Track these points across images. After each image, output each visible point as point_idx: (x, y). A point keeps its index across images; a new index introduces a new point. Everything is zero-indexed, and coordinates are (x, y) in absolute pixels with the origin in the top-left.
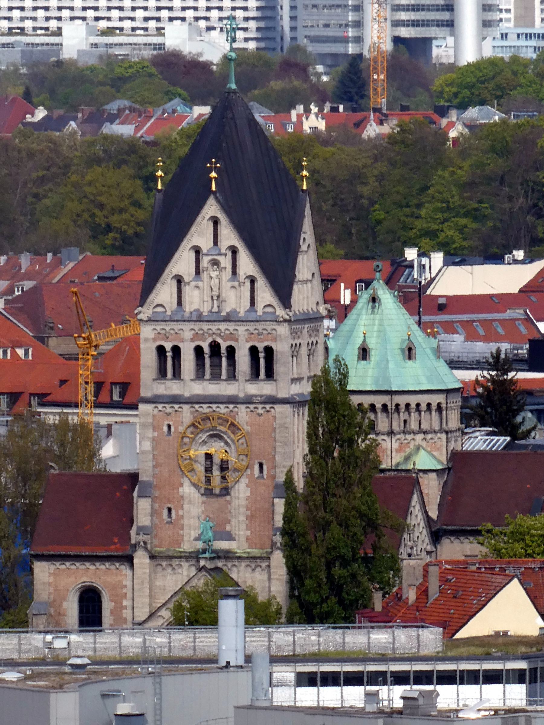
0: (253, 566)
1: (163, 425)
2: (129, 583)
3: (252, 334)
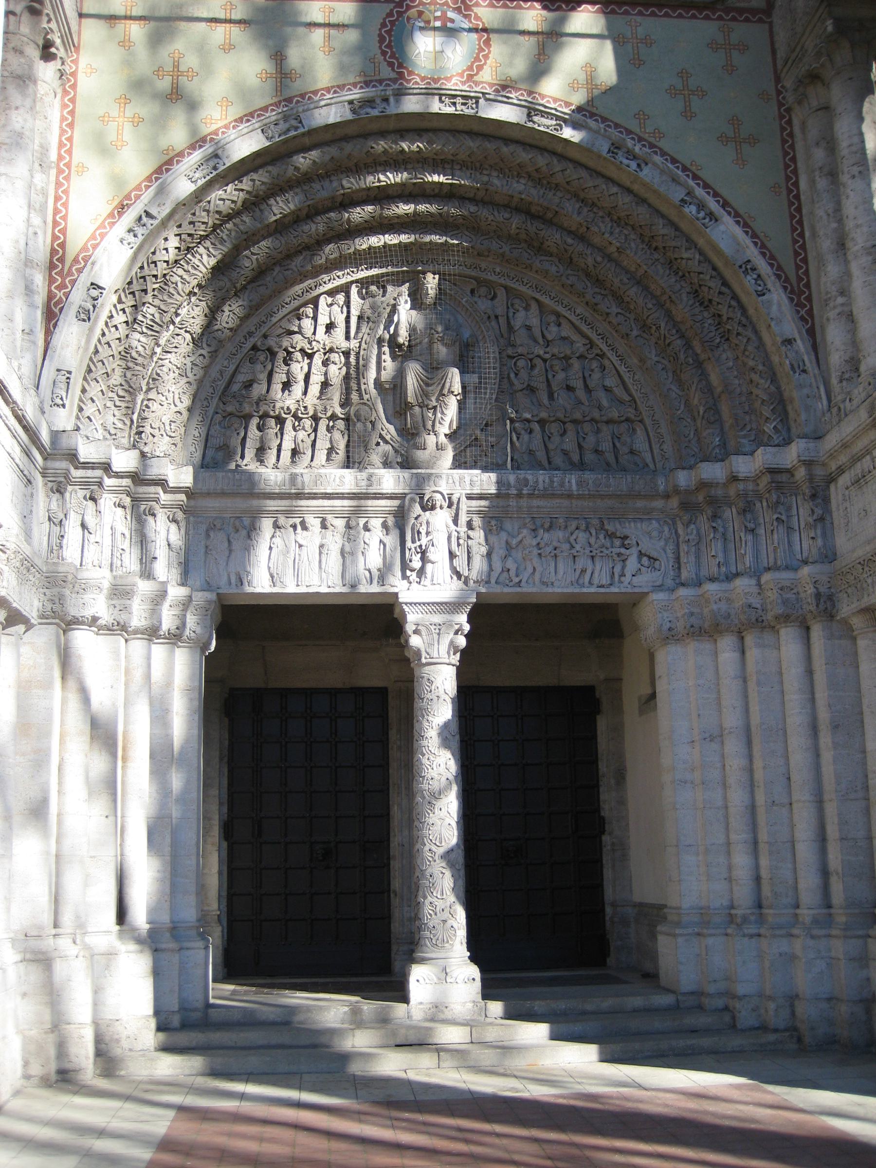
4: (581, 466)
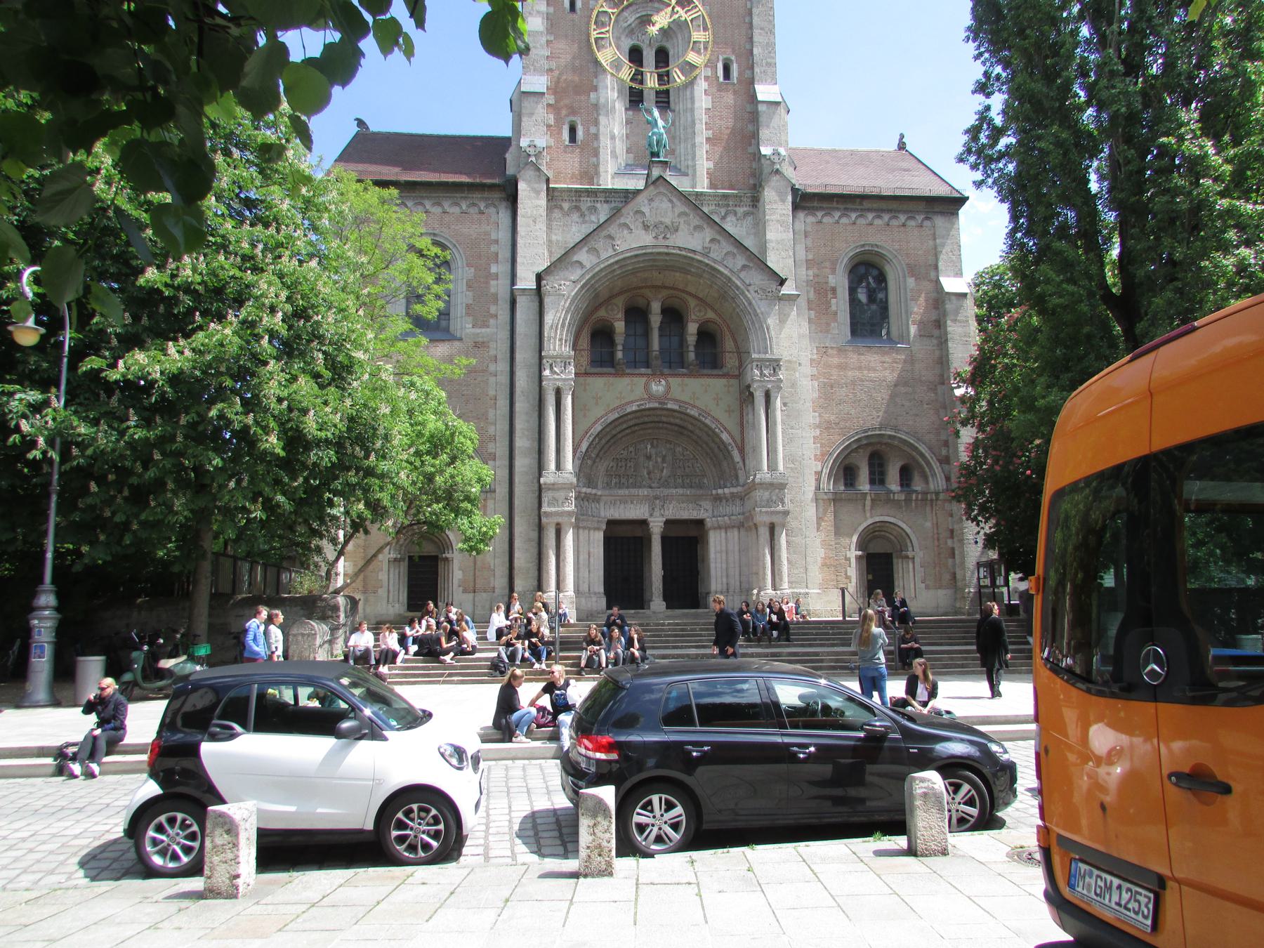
0: (723, 211)
2: (503, 235)
4: (691, 487)
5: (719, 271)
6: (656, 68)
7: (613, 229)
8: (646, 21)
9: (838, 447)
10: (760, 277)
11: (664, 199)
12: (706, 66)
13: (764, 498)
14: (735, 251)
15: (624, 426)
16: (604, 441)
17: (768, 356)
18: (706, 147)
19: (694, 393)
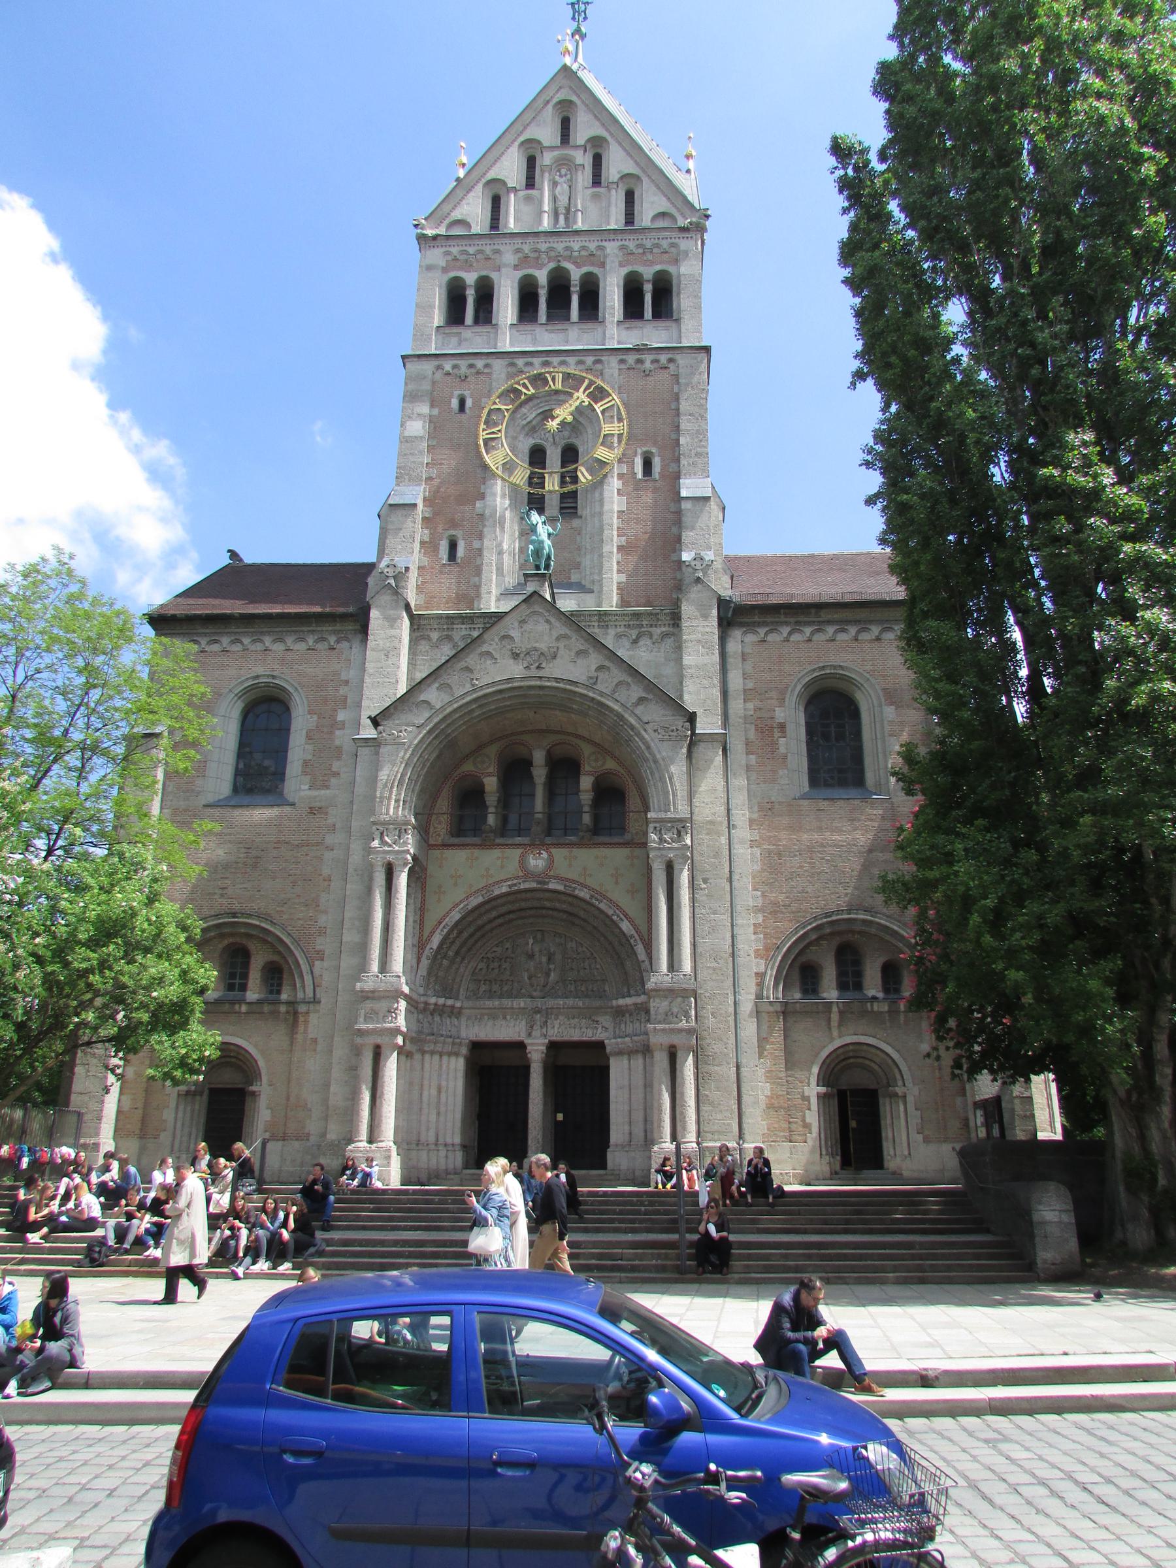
1: (451, 397)
3: (633, 254)
4: (587, 996)
5: (608, 707)
6: (562, 467)
7: (471, 660)
8: (548, 415)
9: (788, 938)
10: (662, 712)
11: (541, 620)
12: (620, 461)
13: (661, 1011)
14: (629, 680)
15: (494, 914)
16: (465, 935)
17: (669, 815)
18: (616, 557)
19: (585, 869)
